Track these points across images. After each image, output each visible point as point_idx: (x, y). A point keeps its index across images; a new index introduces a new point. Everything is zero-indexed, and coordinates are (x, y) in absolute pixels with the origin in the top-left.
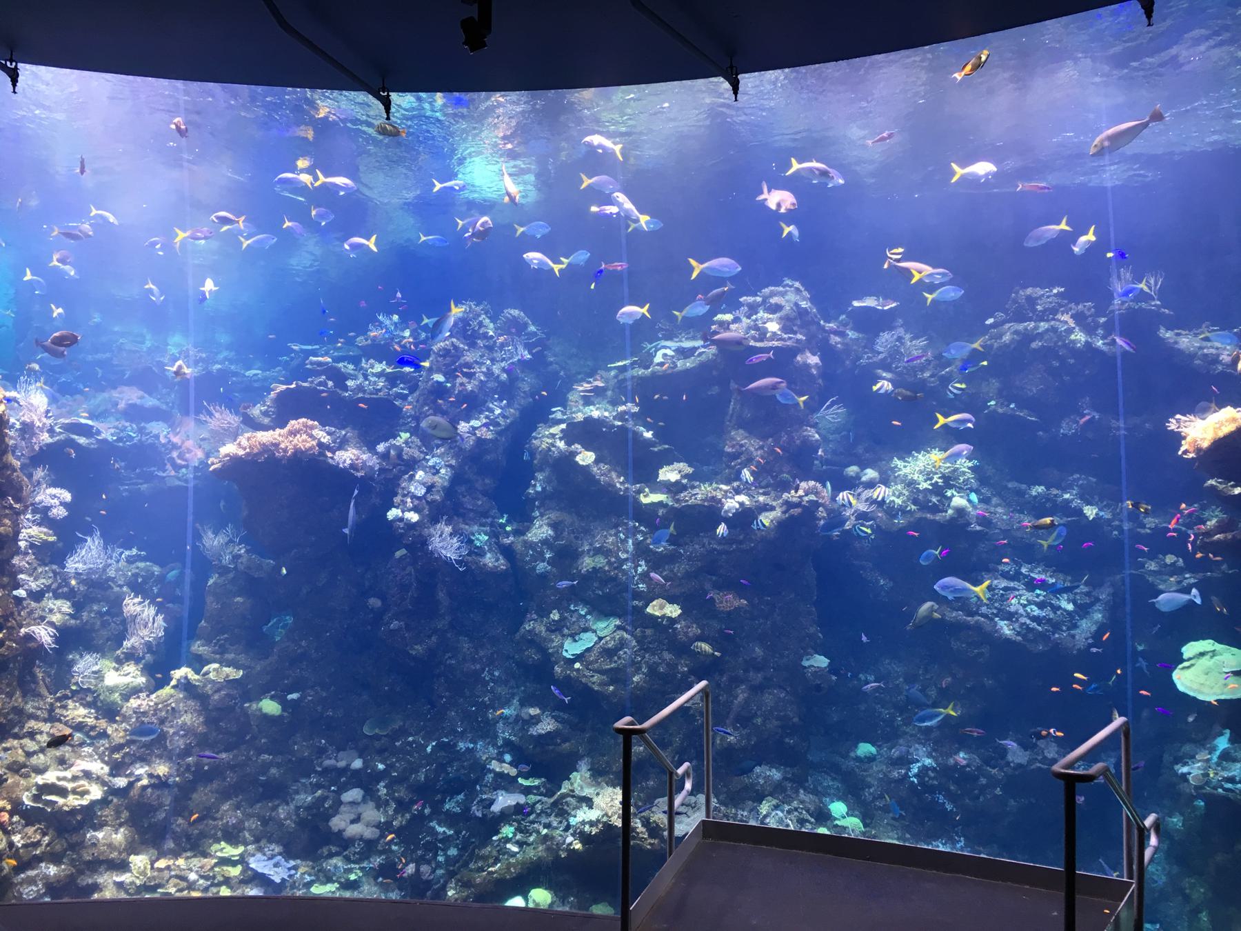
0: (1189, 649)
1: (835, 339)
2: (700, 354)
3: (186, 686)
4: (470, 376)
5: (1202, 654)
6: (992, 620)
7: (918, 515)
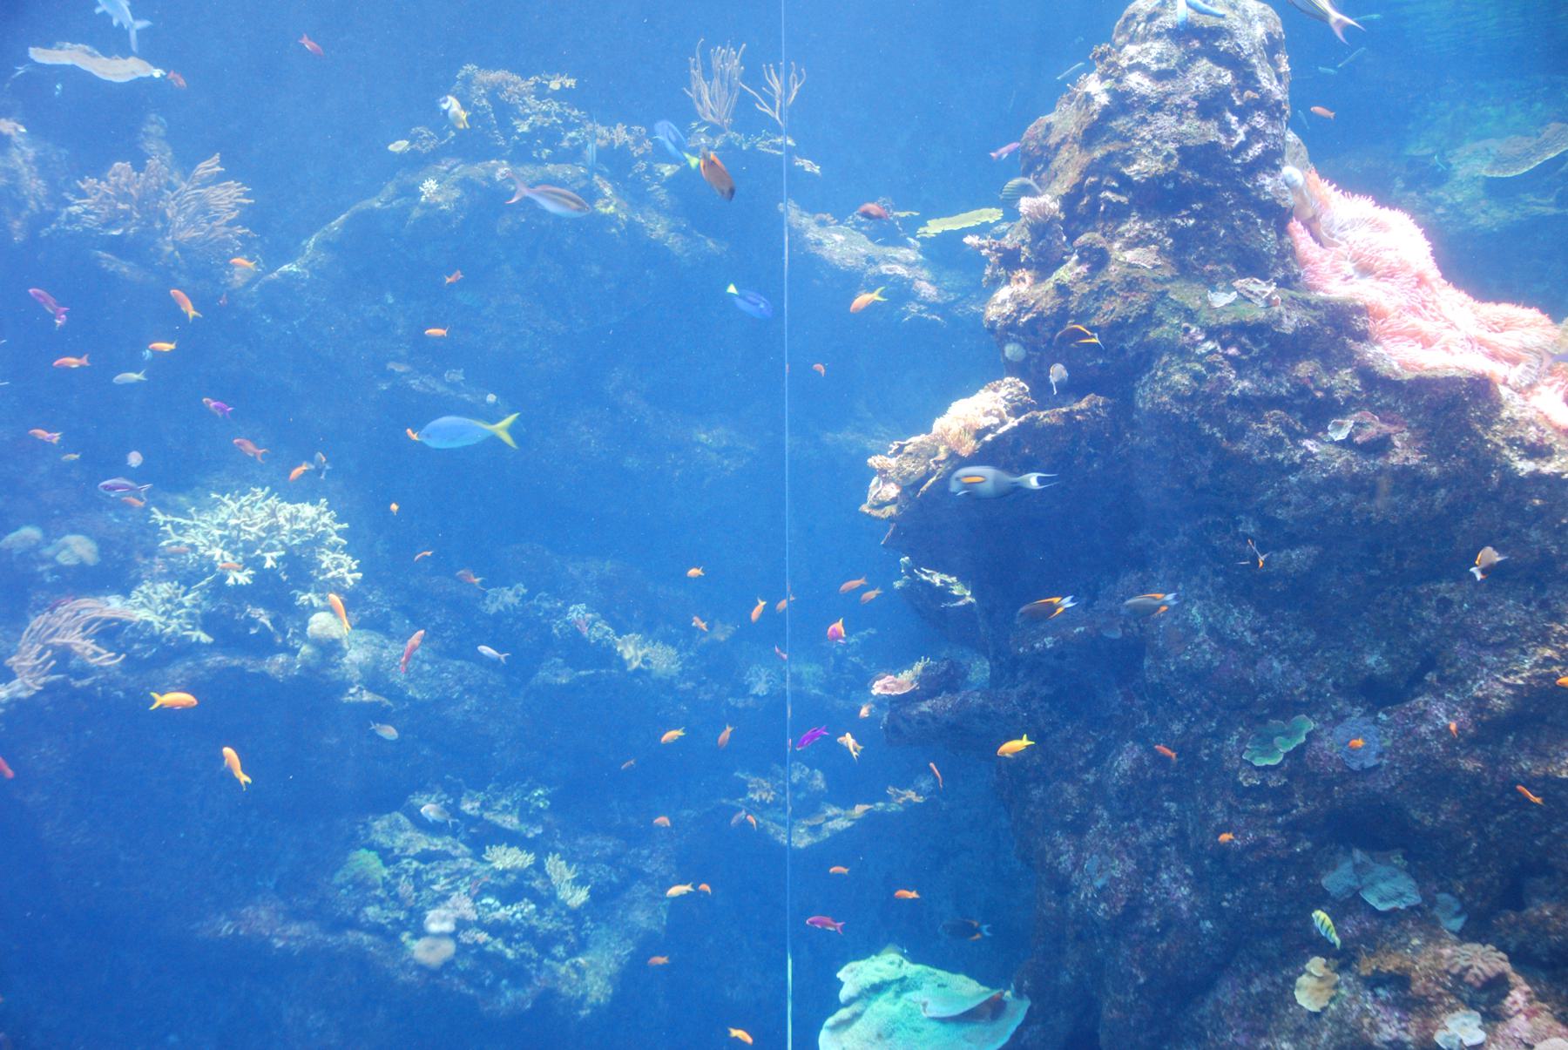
0: (854, 976)
5: (877, 989)
6: (393, 937)
7: (216, 660)
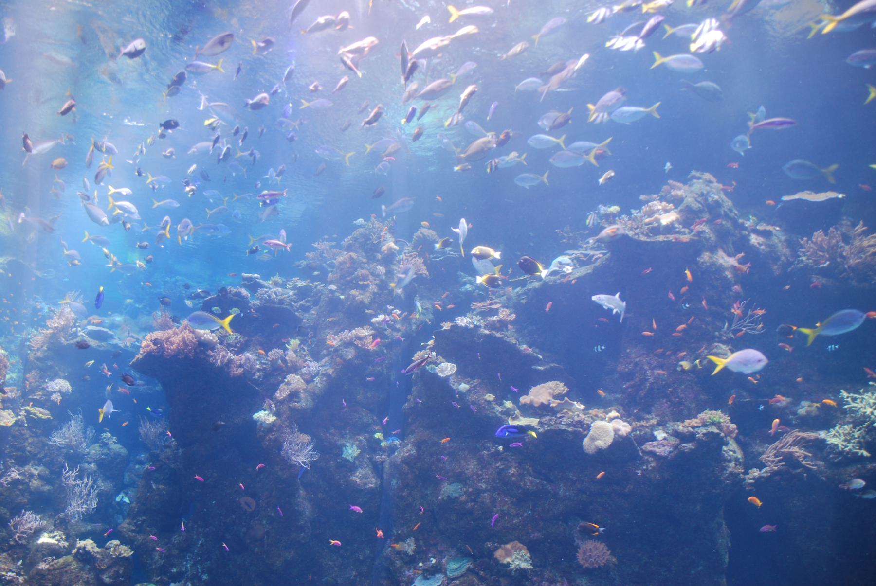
1: (754, 239)
2: (597, 259)
3: (85, 557)
4: (364, 288)
